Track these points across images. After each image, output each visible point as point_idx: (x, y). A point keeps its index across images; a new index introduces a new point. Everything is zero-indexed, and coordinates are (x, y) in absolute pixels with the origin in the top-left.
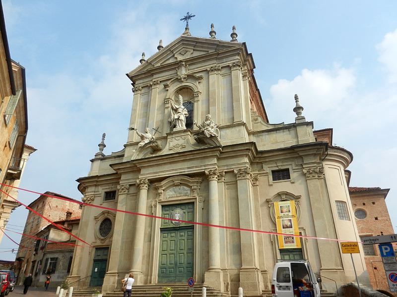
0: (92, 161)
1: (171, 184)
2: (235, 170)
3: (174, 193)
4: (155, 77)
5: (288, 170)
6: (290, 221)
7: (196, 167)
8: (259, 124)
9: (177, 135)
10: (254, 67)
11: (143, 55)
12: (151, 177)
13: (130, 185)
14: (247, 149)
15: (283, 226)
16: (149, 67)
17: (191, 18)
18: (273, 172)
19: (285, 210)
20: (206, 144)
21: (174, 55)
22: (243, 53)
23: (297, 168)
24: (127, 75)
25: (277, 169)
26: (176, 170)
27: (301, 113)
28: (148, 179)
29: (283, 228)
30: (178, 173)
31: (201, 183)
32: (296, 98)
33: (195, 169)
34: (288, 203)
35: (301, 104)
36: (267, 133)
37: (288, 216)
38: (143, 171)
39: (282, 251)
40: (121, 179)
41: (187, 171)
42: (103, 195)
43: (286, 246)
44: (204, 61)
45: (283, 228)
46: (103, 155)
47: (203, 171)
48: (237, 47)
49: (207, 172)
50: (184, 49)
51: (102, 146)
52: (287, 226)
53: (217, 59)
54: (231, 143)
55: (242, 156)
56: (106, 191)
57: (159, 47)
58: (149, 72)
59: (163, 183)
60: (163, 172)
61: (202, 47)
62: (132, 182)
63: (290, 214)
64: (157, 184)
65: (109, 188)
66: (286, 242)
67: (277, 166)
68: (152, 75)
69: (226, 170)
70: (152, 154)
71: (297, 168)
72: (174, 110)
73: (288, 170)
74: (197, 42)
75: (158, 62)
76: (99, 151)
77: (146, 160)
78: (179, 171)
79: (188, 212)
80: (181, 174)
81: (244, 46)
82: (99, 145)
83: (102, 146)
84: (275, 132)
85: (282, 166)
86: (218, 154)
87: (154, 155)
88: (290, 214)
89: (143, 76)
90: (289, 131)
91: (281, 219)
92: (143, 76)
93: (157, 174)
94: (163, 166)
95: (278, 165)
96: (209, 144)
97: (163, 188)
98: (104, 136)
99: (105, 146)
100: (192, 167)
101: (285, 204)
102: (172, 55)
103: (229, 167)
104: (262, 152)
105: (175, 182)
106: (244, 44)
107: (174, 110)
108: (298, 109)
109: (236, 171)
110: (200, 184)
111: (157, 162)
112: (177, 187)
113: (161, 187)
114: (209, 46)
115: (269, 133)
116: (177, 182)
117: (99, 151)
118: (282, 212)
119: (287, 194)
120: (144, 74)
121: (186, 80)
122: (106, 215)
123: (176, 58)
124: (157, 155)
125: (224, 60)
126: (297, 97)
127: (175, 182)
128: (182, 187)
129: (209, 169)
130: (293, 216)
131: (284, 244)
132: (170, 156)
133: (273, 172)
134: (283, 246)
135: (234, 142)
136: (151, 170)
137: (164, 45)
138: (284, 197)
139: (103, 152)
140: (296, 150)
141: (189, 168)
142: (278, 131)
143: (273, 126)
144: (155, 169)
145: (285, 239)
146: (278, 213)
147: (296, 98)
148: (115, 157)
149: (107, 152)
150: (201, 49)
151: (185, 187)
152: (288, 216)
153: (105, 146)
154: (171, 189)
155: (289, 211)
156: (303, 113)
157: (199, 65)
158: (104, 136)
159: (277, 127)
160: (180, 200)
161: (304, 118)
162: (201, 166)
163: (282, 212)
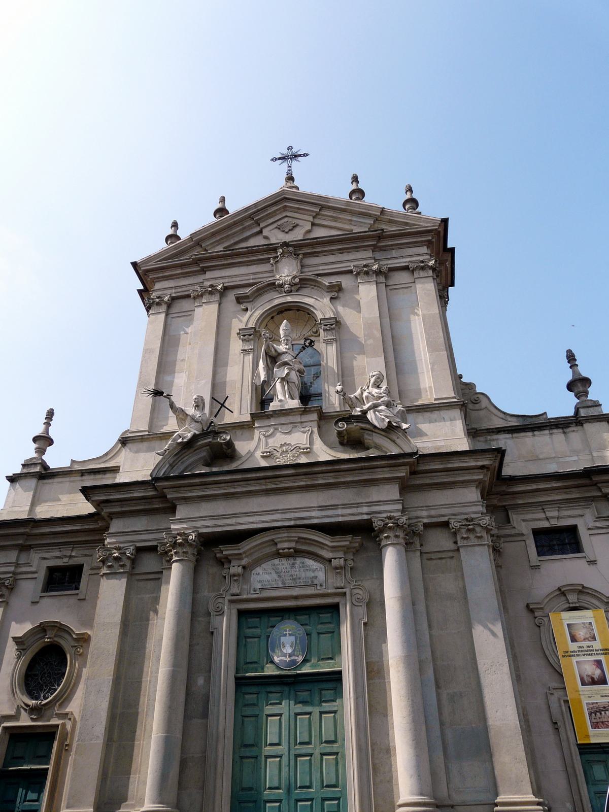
0: (12, 479)
1: (268, 550)
2: (452, 521)
3: (275, 576)
4: (209, 275)
5: (573, 529)
6: (599, 663)
7: (345, 506)
8: (485, 411)
9: (283, 420)
10: (452, 285)
11: (175, 225)
12: (208, 527)
13: (140, 550)
14: (482, 467)
15: (582, 679)
16: (197, 253)
17: (299, 158)
18: (537, 533)
19: (581, 633)
20: (368, 449)
21: (261, 232)
22: (439, 240)
23: (598, 524)
24: (134, 265)
25: (546, 524)
26: (285, 511)
27: (587, 393)
28: (200, 535)
29: (583, 684)
30: (290, 520)
31: (357, 552)
32: (571, 358)
33: (340, 512)
34: (586, 616)
35: (584, 372)
36: (509, 436)
37: (589, 652)
38: (182, 511)
39: (587, 750)
40: (112, 530)
41: (317, 517)
42: (42, 575)
43: (597, 735)
44: (342, 251)
45: (583, 684)
46: (45, 466)
47: (366, 517)
48: (427, 226)
49: (377, 524)
50: (286, 220)
51: (44, 441)
52: (593, 679)
53: (375, 248)
54: (435, 448)
55: (466, 484)
56: (52, 563)
57: (221, 211)
58: (196, 262)
59: (246, 546)
60: (247, 514)
61: (335, 219)
62: (147, 539)
63: (597, 645)
64: (228, 551)
65: (61, 558)
66: (595, 726)
67: (547, 519)
68: (204, 271)
69: (426, 521)
70: (208, 465)
71: (598, 524)
72: (270, 357)
73: (573, 529)
74: (322, 207)
75: (219, 242)
76: (35, 455)
77: (197, 480)
78: (293, 515)
79: (319, 634)
80: (298, 522)
81: (443, 223)
82: (35, 440)
83: (44, 441)
84: (530, 434)
85: (558, 518)
86: (402, 473)
87: (215, 469)
88: (597, 645)
89: (179, 271)
90: (564, 433)
91: (574, 659)
92: (179, 271)
93: (233, 521)
94: (244, 501)
95: (549, 514)
96: (377, 447)
97: (244, 562)
98: (50, 414)
99: (50, 442)
100: (334, 507)
101: (580, 617)
102: (258, 229)
103: (433, 513)
104: (513, 480)
105: (280, 546)
106: (445, 222)
107: (270, 357)
108: (579, 385)
109: (454, 524)
110: (354, 554)
111: (246, 485)
112: (284, 561)
113: (239, 556)
114: (354, 219)
115: (515, 435)
116: (286, 545)
117: (35, 455)
118: (574, 639)
119: (582, 591)
120: (182, 266)
121: (297, 291)
122: (50, 633)
123: (266, 238)
124: (226, 468)
125: (394, 253)
126: (573, 355)
127: (280, 546)
128: (299, 561)
129: (380, 512)
130: (568, 654)
131: (591, 731)
132: (270, 474)
133: (537, 533)
134: (588, 736)
135: (440, 447)
136: (206, 509)
137: (233, 207)
138: (572, 598)
139: (44, 457)
140: (596, 478)
141: (322, 508)
142: (536, 433)
143: (521, 419)
144: (220, 507)
145: (590, 714)
146: (564, 643)
147: (571, 358)
148: (83, 473)
149: (55, 459)
150: (333, 224)
151: (310, 562)
152: (589, 652)
153: (50, 442)
154: (267, 565)
155: (594, 638)
156: (593, 394)
157: (331, 259)
158: (50, 414)
159: (529, 421)
160: (296, 598)
161: (597, 405)
162: (358, 505)
163: (574, 639)
